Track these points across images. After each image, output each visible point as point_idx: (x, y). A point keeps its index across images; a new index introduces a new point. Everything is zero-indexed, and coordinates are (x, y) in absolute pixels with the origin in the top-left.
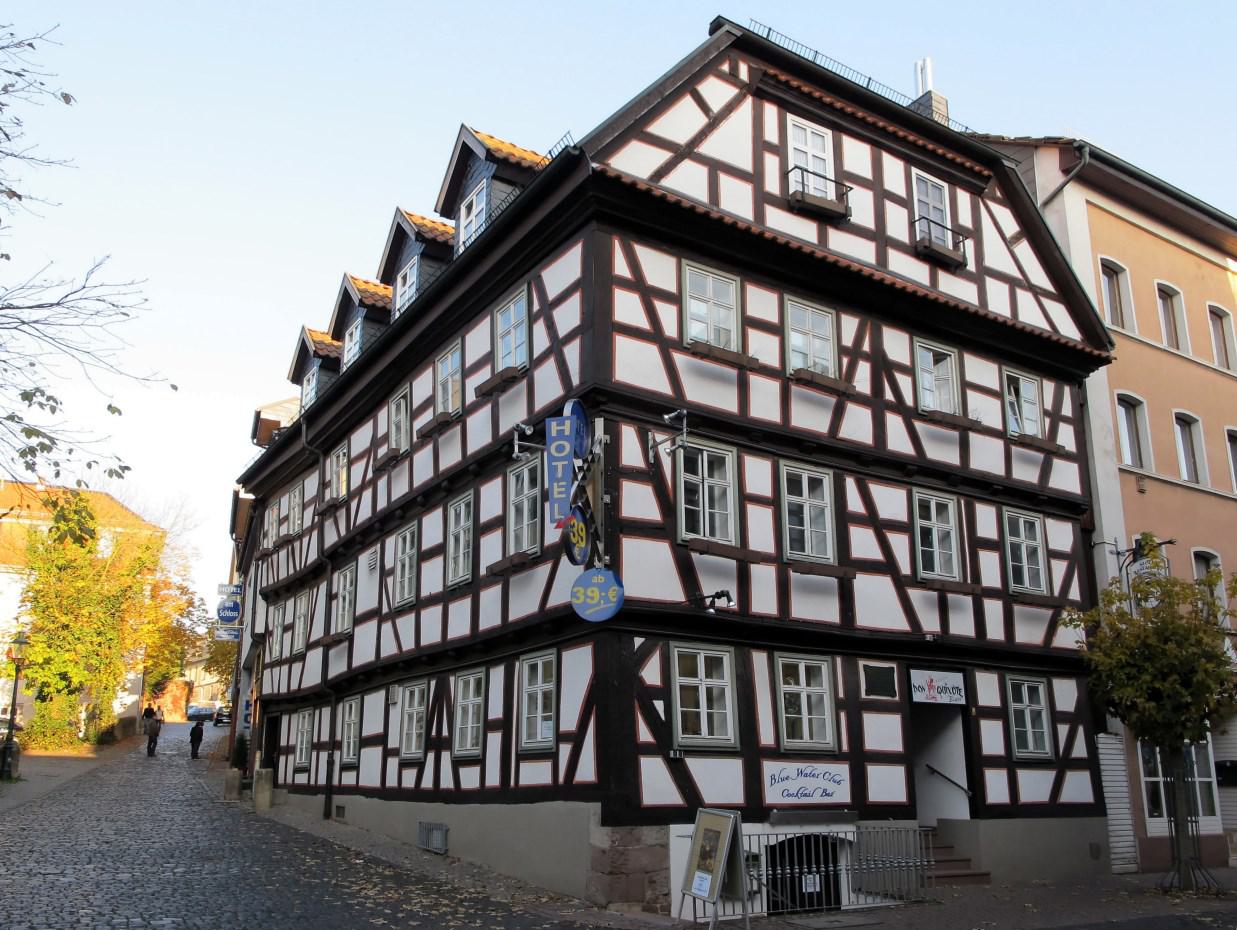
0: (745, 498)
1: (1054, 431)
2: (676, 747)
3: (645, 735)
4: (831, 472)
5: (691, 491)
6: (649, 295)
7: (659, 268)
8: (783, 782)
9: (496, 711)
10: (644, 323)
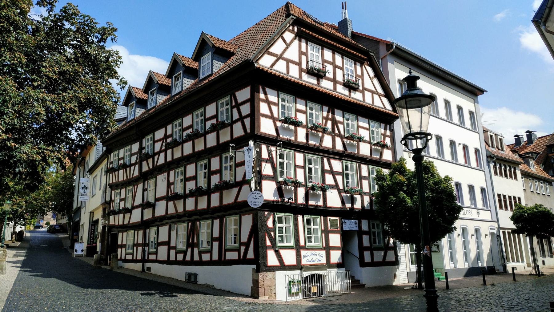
1: (384, 139)
3: (268, 243)
5: (282, 164)
6: (269, 103)
8: (307, 257)
9: (216, 234)
10: (268, 113)
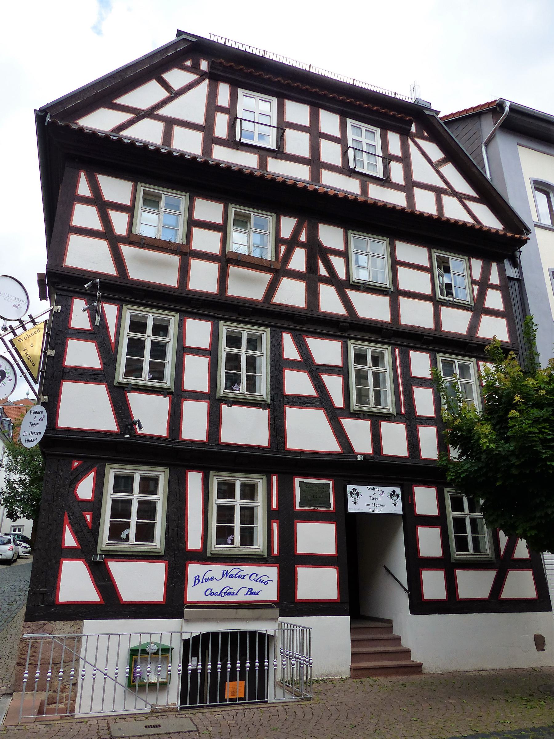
0: (183, 350)
2: (99, 551)
4: (268, 330)
7: (115, 189)
